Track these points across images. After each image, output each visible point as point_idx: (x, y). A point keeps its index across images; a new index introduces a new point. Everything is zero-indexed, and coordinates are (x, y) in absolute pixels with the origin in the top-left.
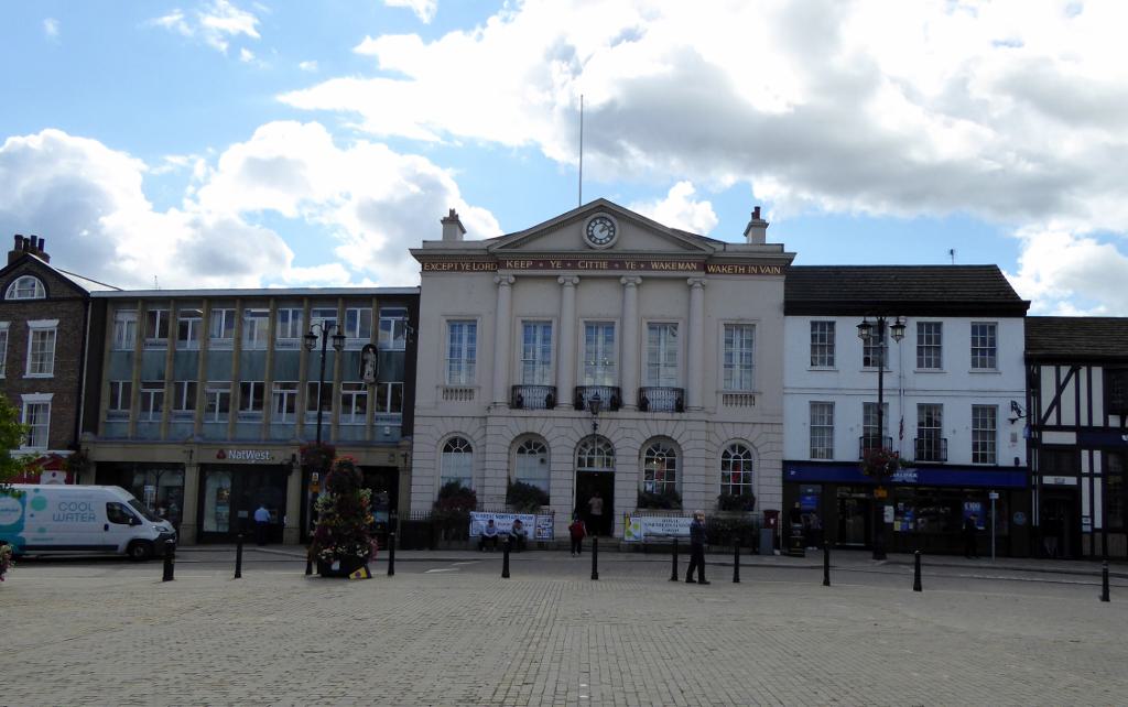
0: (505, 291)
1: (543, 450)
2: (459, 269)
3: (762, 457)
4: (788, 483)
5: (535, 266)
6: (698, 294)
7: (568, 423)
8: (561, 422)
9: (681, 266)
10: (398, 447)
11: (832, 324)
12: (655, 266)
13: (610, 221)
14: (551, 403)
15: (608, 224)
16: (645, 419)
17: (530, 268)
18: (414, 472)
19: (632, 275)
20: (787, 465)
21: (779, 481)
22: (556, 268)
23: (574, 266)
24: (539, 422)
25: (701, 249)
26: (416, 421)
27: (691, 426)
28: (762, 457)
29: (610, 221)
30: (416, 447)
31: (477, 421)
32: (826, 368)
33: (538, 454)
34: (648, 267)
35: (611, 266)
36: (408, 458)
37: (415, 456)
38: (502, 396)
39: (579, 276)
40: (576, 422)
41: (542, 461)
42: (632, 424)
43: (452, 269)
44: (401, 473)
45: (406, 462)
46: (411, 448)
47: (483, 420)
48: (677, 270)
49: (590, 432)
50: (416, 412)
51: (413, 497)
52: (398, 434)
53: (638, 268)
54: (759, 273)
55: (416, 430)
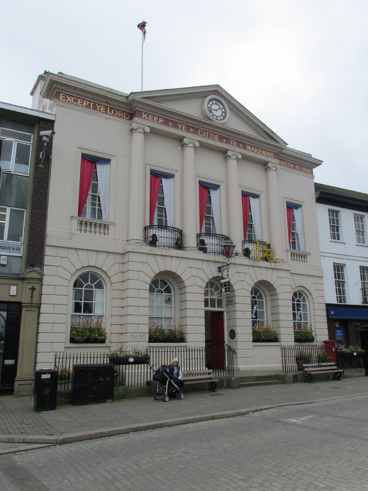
0: (138, 137)
1: (168, 290)
2: (95, 108)
3: (315, 300)
4: (330, 321)
5: (166, 122)
6: (272, 174)
7: (198, 264)
8: (192, 263)
9: (264, 153)
10: (23, 279)
11: (337, 212)
12: (248, 148)
13: (222, 104)
14: (179, 245)
15: (221, 107)
16: (253, 266)
17: (162, 123)
18: (43, 309)
19: (234, 150)
20: (329, 306)
21: (325, 319)
22: (181, 129)
23: (196, 131)
24: (176, 261)
25: (280, 143)
26: (48, 251)
27: (282, 274)
28: (315, 300)
29: (222, 104)
30: (46, 280)
31: (111, 256)
32: (336, 240)
33: (164, 293)
34: (244, 146)
35: (221, 138)
36: (36, 292)
37: (45, 289)
38: (137, 234)
39: (199, 141)
40: (205, 265)
41: (169, 300)
42: (245, 269)
43: (88, 107)
44: (24, 310)
45: (32, 297)
46: (40, 280)
47: (119, 259)
48: (262, 154)
49: (216, 274)
50: (49, 241)
51: (41, 338)
52: (17, 267)
53: (239, 147)
54: (301, 170)
55: (47, 260)
